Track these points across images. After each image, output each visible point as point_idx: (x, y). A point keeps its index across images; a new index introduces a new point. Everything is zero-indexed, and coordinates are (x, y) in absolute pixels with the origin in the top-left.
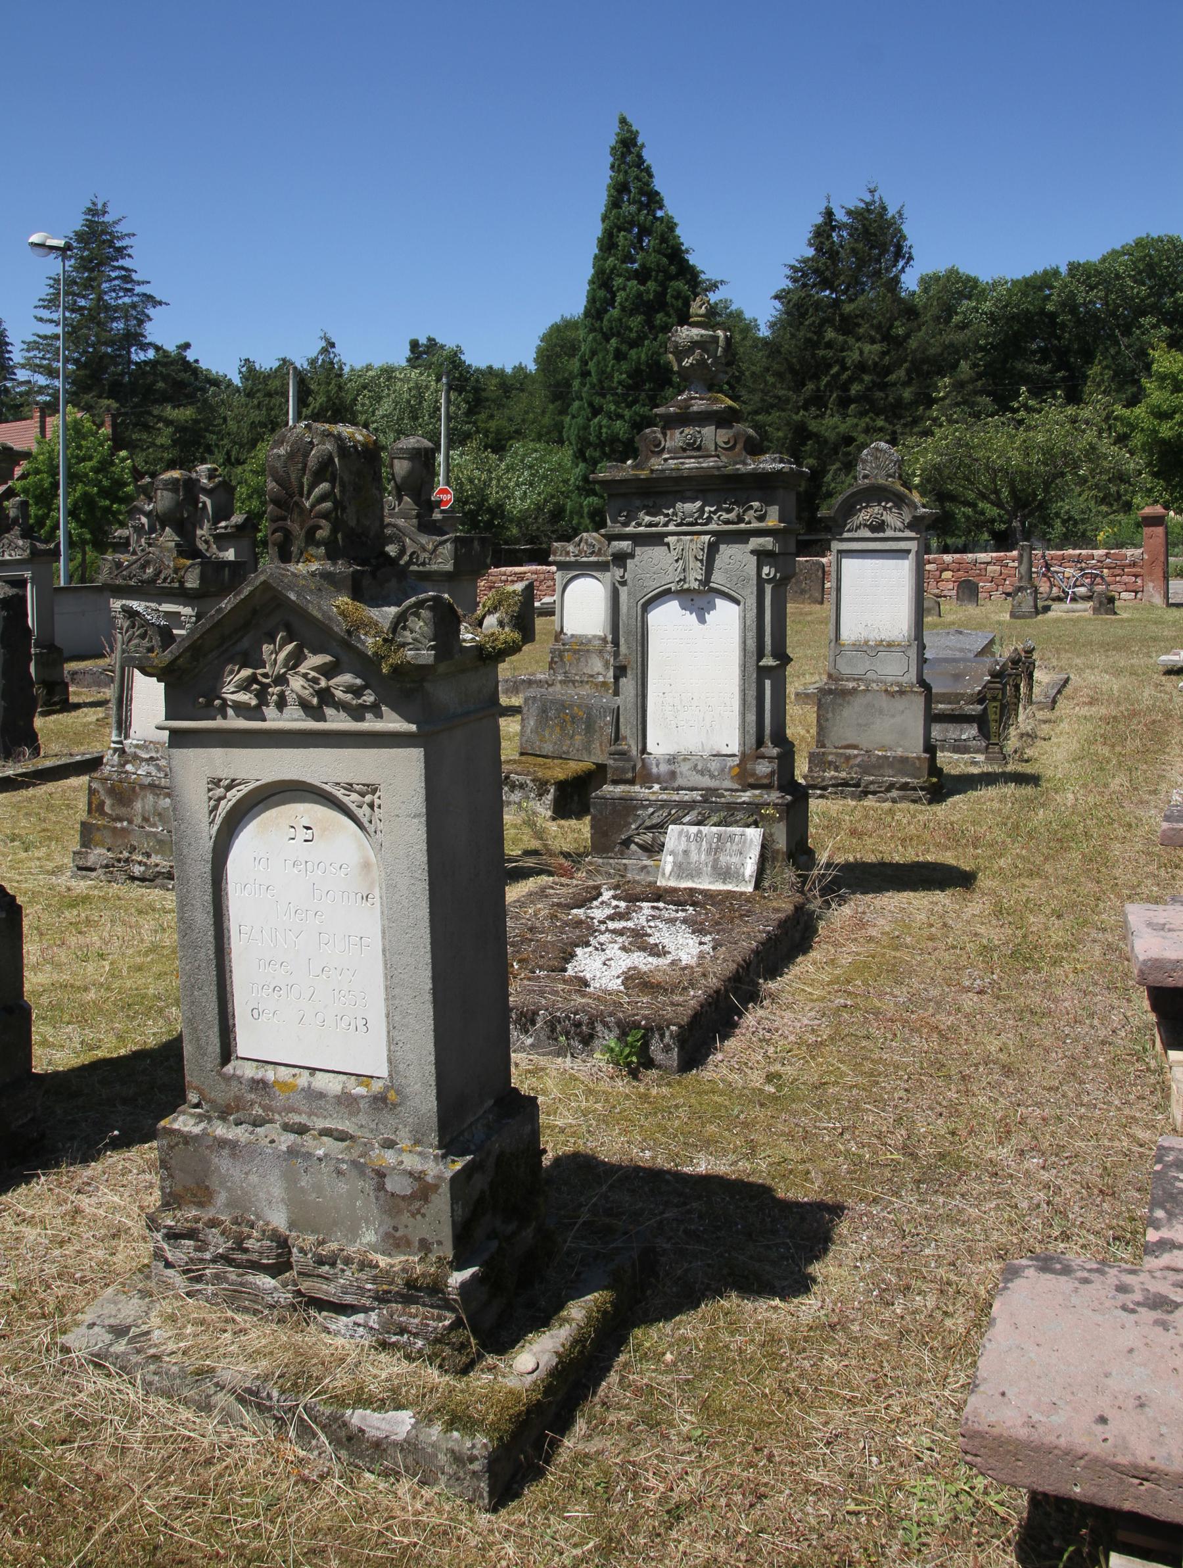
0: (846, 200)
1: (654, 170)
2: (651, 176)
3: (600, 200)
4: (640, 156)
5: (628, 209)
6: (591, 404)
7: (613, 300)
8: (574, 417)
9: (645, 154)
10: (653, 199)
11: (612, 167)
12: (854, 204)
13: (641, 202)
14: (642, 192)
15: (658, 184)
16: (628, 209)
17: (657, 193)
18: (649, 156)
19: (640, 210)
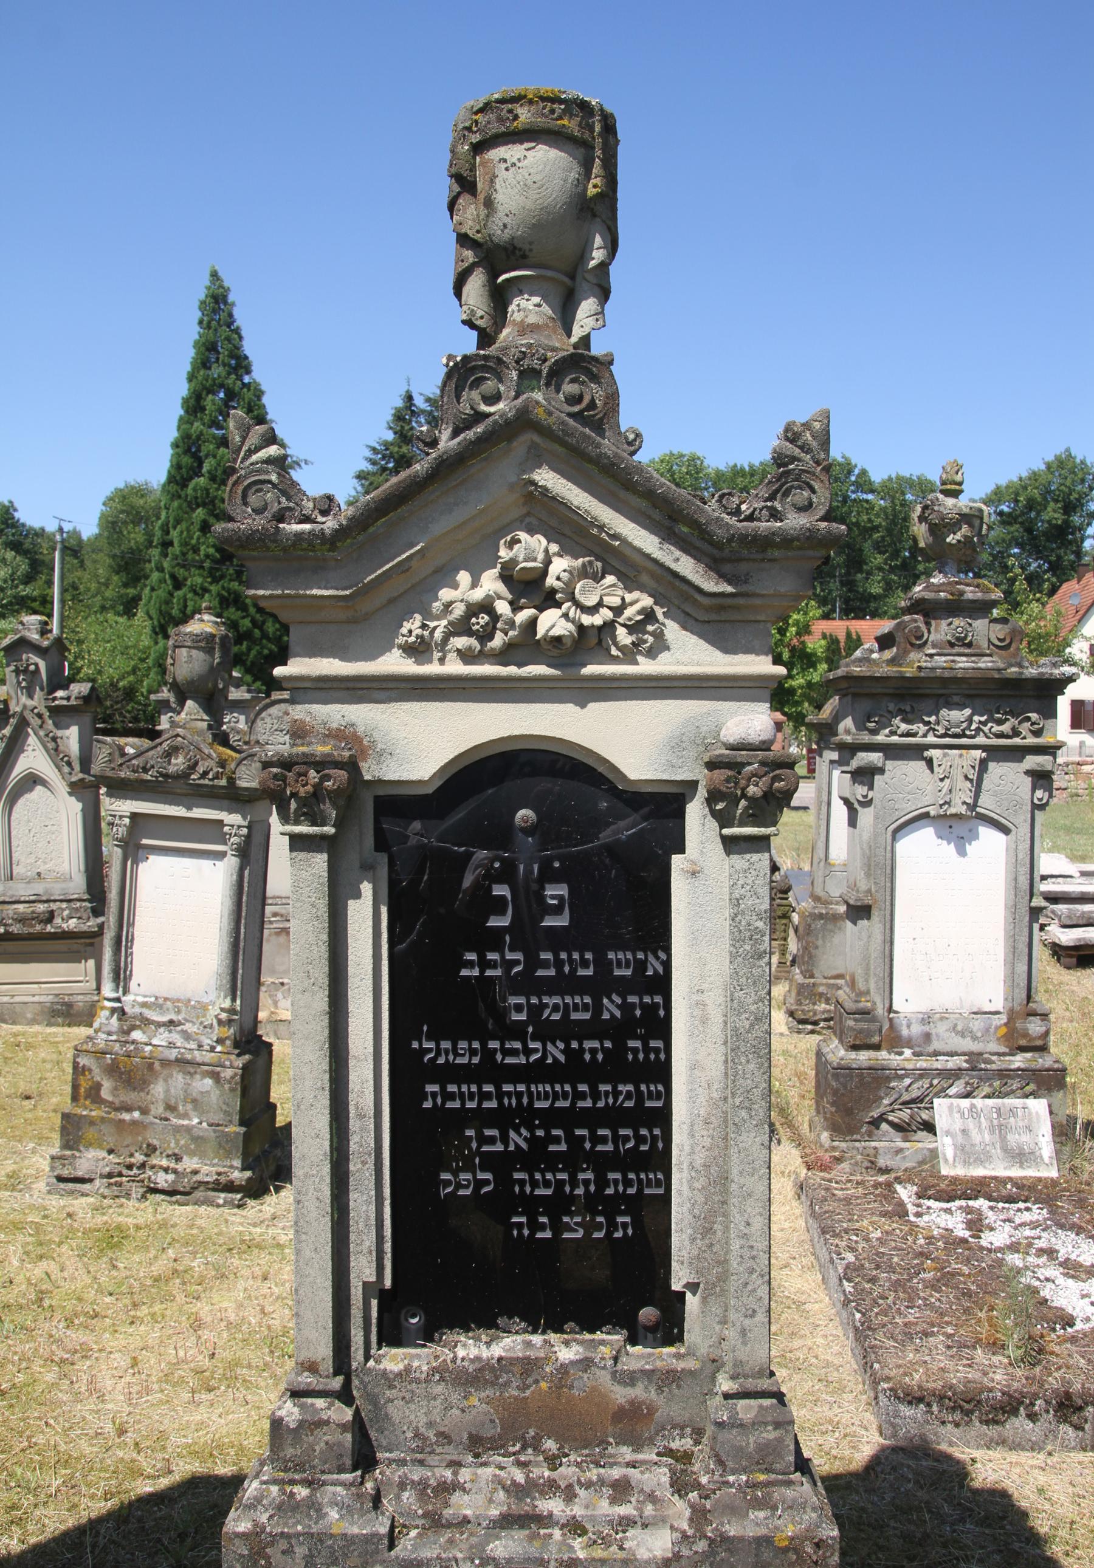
1: (243, 333)
2: (241, 338)
3: (185, 356)
4: (231, 315)
5: (217, 371)
6: (173, 577)
7: (200, 466)
8: (153, 589)
9: (236, 313)
10: (241, 364)
11: (201, 322)
13: (230, 365)
14: (232, 356)
15: (249, 348)
16: (217, 371)
17: (246, 358)
19: (229, 374)
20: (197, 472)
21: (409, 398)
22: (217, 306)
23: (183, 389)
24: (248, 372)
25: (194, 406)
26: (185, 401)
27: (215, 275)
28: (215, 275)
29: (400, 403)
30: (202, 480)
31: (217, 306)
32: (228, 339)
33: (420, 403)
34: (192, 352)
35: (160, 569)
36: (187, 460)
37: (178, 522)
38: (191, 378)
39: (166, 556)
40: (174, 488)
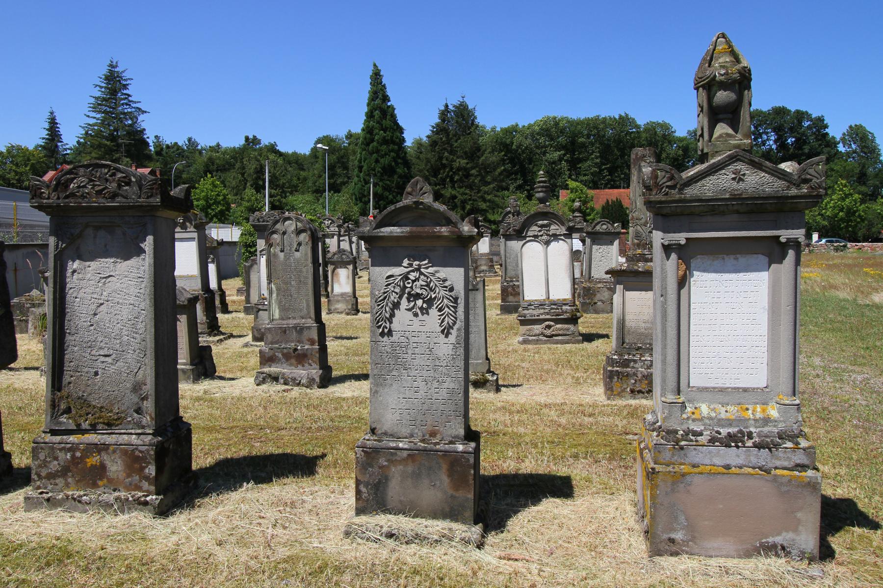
0: (453, 102)
6: (364, 180)
10: (386, 98)
12: (456, 103)
18: (384, 81)
20: (372, 141)
21: (447, 106)
22: (377, 77)
23: (365, 109)
24: (389, 101)
25: (370, 115)
26: (367, 114)
27: (375, 65)
28: (375, 65)
29: (443, 108)
30: (375, 143)
31: (377, 77)
32: (382, 90)
33: (451, 107)
34: (368, 95)
35: (358, 176)
36: (368, 136)
37: (365, 159)
38: (368, 105)
39: (361, 172)
40: (363, 146)
